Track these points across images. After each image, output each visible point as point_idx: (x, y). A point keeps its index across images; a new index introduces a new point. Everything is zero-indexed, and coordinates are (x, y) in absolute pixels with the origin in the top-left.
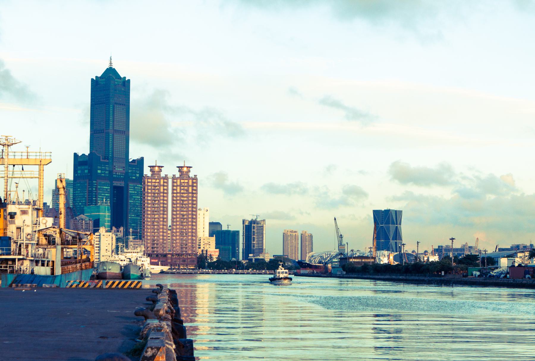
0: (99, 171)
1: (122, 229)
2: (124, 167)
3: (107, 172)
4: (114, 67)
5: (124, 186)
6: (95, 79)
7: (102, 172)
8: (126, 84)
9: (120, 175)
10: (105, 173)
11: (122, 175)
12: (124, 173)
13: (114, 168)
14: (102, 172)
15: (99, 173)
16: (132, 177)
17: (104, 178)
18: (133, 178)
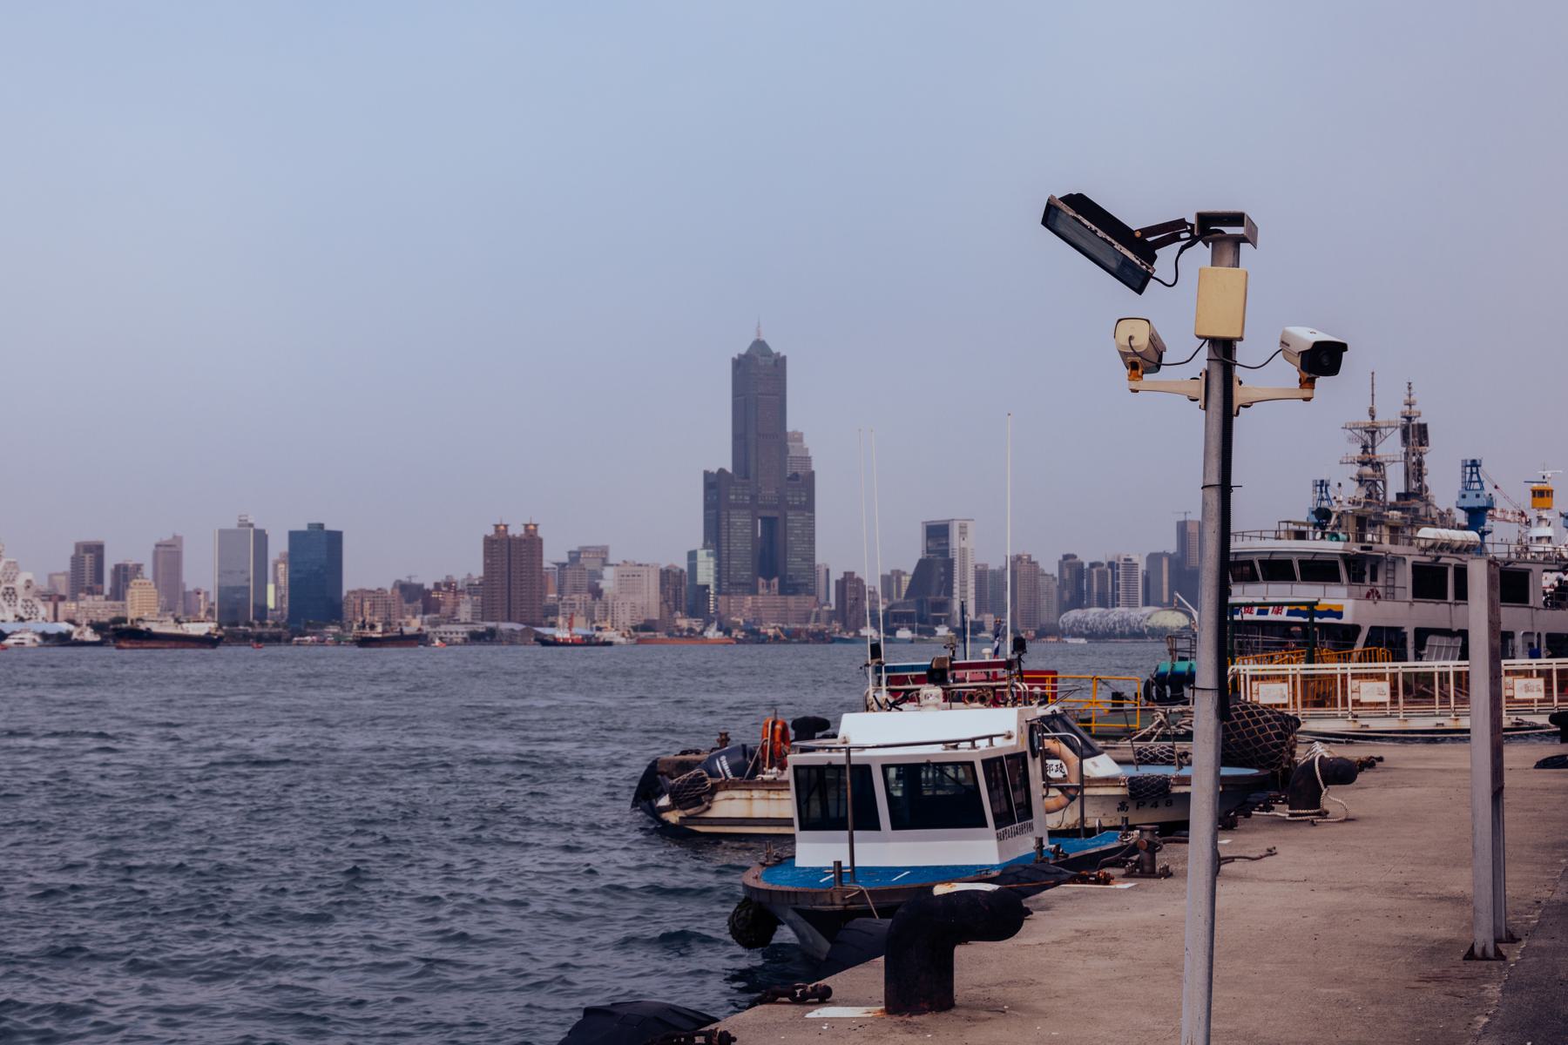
1: (776, 581)
3: (747, 498)
4: (763, 338)
6: (736, 357)
8: (780, 363)
10: (743, 500)
17: (743, 507)
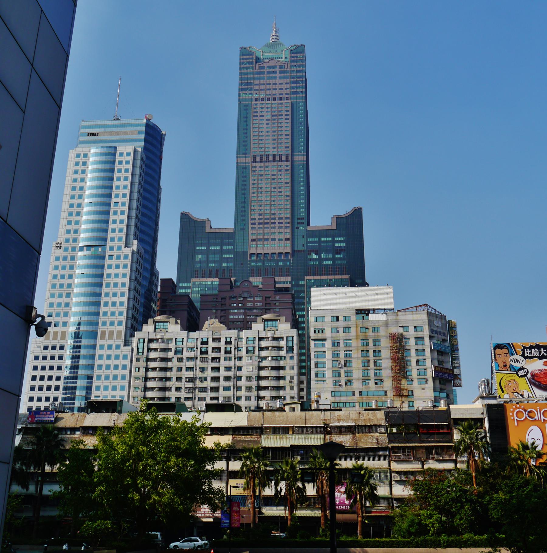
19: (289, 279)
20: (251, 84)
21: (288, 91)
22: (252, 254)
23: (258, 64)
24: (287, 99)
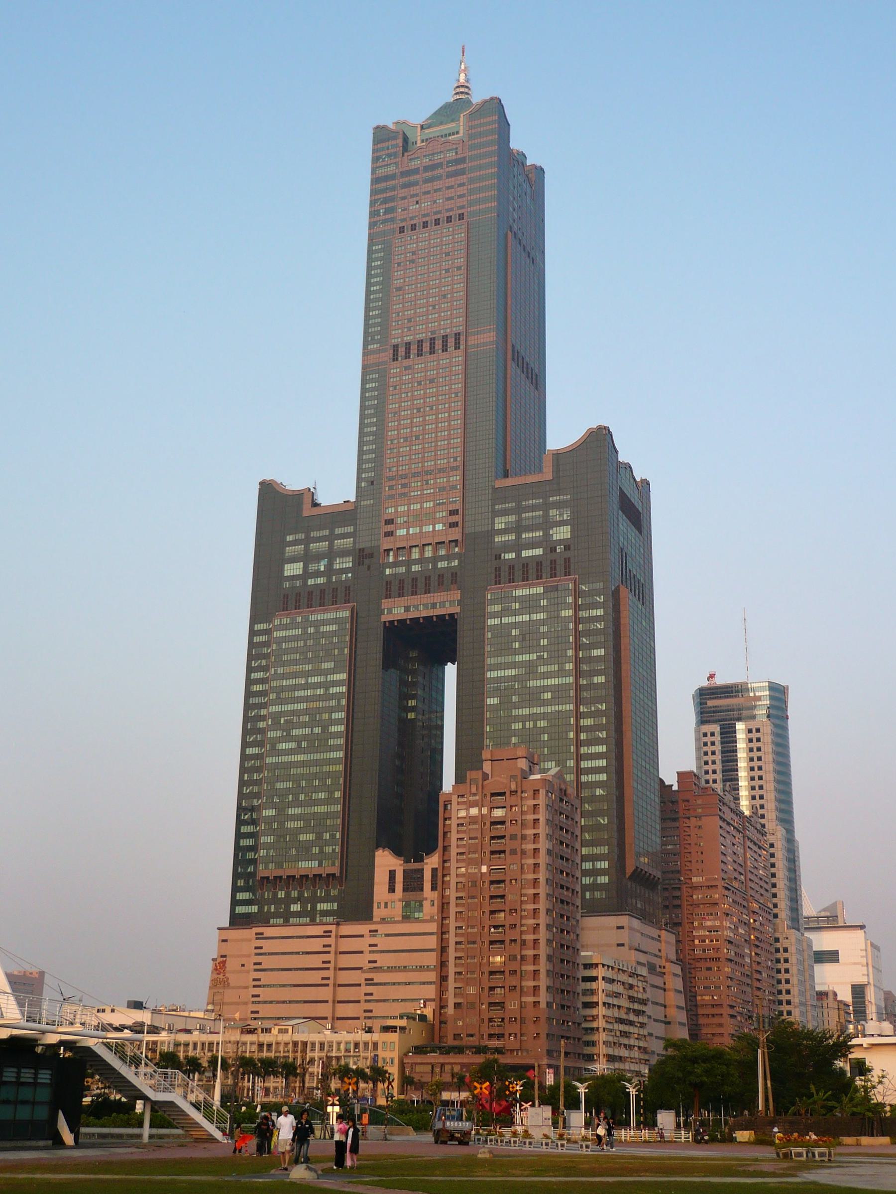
0: (293, 569)
2: (453, 513)
5: (456, 609)
7: (312, 567)
9: (435, 559)
11: (448, 558)
12: (456, 541)
13: (389, 528)
14: (312, 567)
15: (293, 578)
16: (518, 547)
18: (525, 553)
19: (456, 595)
20: (392, 199)
21: (463, 201)
22: (385, 550)
23: (406, 154)
24: (461, 217)
